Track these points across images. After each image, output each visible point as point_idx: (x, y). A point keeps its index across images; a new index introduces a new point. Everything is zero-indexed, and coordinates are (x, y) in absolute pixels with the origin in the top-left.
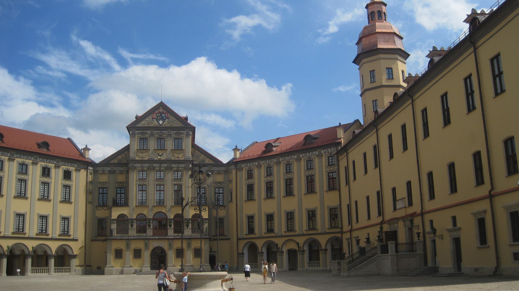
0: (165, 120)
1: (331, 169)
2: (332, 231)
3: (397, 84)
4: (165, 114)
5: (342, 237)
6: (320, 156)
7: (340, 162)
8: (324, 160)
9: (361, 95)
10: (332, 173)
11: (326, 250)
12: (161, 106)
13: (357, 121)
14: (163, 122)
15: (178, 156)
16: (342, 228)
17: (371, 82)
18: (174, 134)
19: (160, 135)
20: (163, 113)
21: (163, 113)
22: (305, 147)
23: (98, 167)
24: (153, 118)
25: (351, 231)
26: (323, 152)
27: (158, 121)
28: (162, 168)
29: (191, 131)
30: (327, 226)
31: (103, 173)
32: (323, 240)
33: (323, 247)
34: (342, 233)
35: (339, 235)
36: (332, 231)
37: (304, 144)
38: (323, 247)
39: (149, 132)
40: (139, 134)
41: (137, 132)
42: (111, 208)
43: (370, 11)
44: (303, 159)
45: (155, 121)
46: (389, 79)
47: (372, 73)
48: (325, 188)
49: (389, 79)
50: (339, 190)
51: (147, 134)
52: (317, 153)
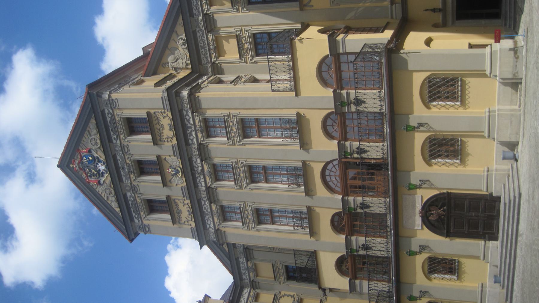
0: (94, 158)
4: (82, 158)
12: (68, 166)
14: (99, 161)
15: (167, 128)
18: (119, 137)
19: (130, 172)
20: (81, 162)
21: (81, 162)
23: (241, 279)
24: (99, 183)
27: (100, 174)
28: (206, 168)
29: (99, 95)
31: (256, 270)
39: (128, 194)
40: (140, 216)
41: (136, 221)
42: (324, 290)
45: (102, 179)
51: (135, 198)
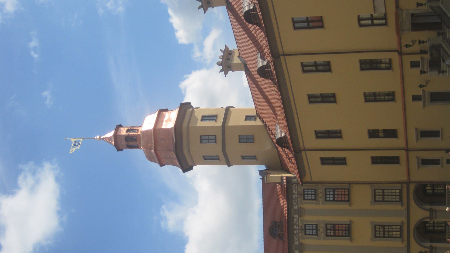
1: (320, 195)
2: (405, 201)
3: (224, 112)
5: (415, 182)
6: (301, 212)
7: (315, 179)
8: (307, 206)
9: (229, 165)
10: (326, 195)
11: (431, 211)
13: (261, 172)
16: (402, 183)
17: (216, 143)
22: (286, 239)
25: (407, 150)
26: (296, 207)
30: (398, 207)
32: (419, 214)
33: (427, 214)
34: (409, 183)
35: (412, 187)
36: (405, 201)
37: (282, 239)
38: (427, 214)
43: (124, 143)
44: (301, 241)
46: (216, 121)
47: (203, 141)
48: (345, 206)
49: (216, 121)
50: (350, 183)
52: (296, 216)
